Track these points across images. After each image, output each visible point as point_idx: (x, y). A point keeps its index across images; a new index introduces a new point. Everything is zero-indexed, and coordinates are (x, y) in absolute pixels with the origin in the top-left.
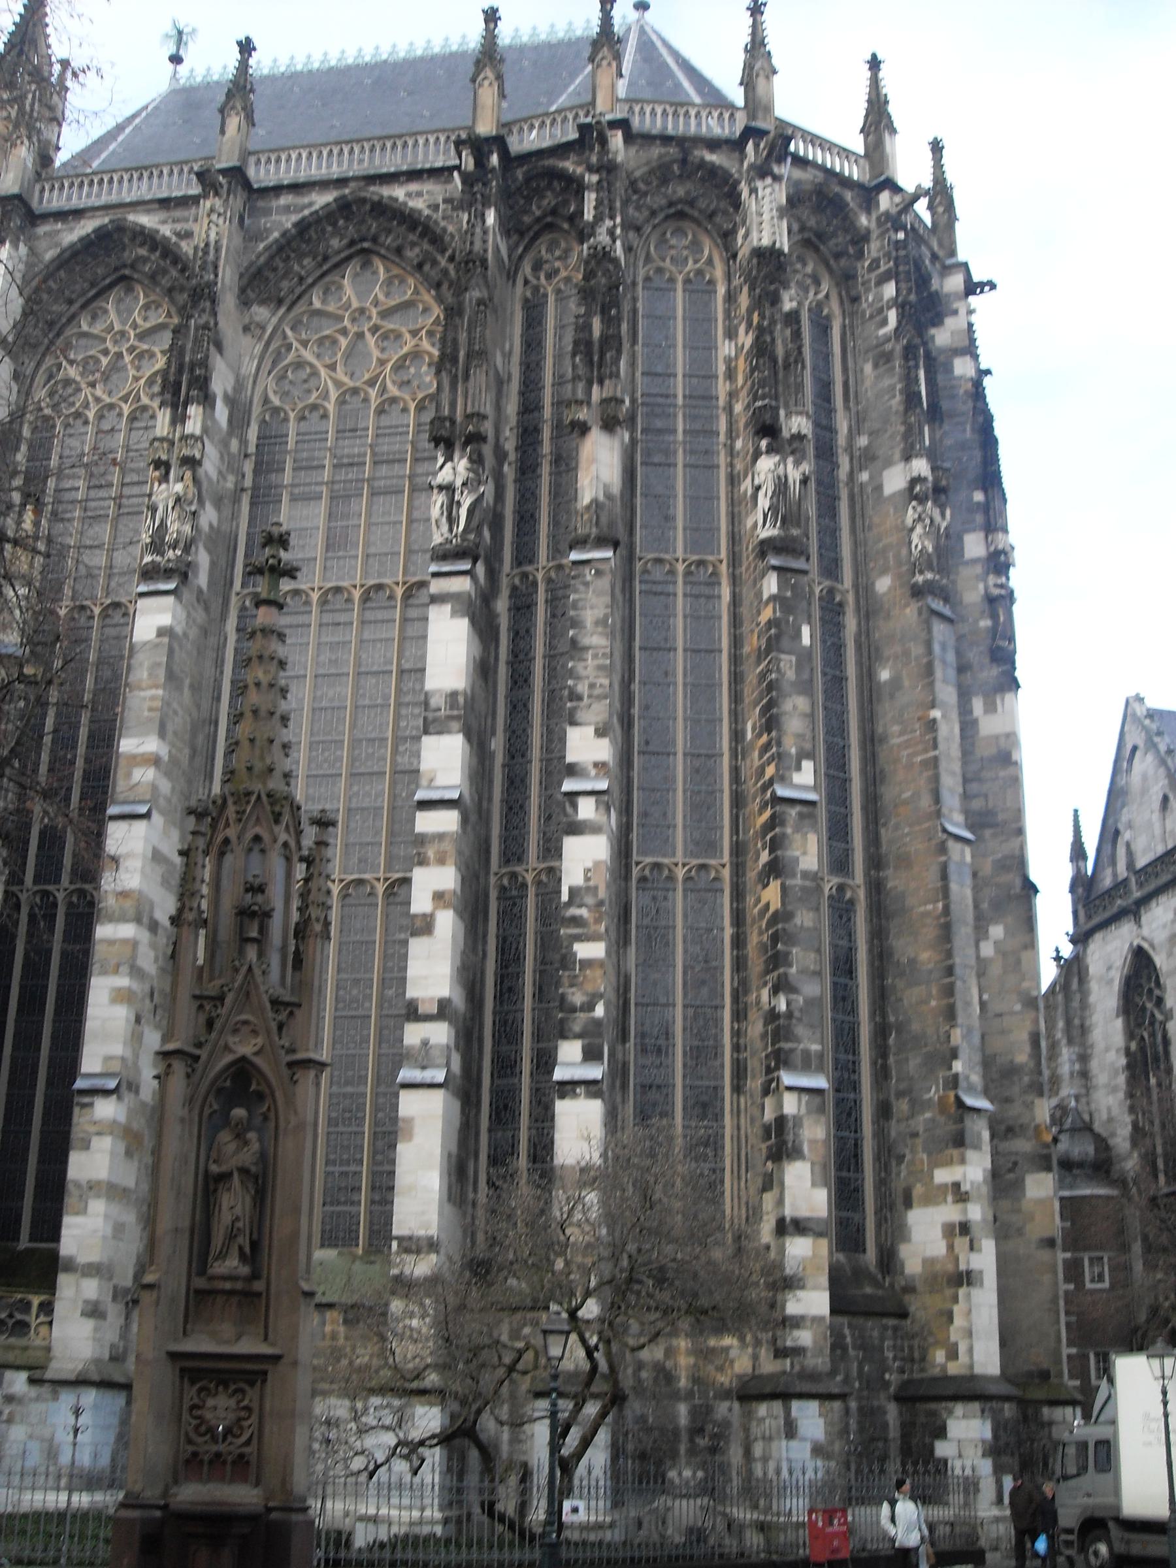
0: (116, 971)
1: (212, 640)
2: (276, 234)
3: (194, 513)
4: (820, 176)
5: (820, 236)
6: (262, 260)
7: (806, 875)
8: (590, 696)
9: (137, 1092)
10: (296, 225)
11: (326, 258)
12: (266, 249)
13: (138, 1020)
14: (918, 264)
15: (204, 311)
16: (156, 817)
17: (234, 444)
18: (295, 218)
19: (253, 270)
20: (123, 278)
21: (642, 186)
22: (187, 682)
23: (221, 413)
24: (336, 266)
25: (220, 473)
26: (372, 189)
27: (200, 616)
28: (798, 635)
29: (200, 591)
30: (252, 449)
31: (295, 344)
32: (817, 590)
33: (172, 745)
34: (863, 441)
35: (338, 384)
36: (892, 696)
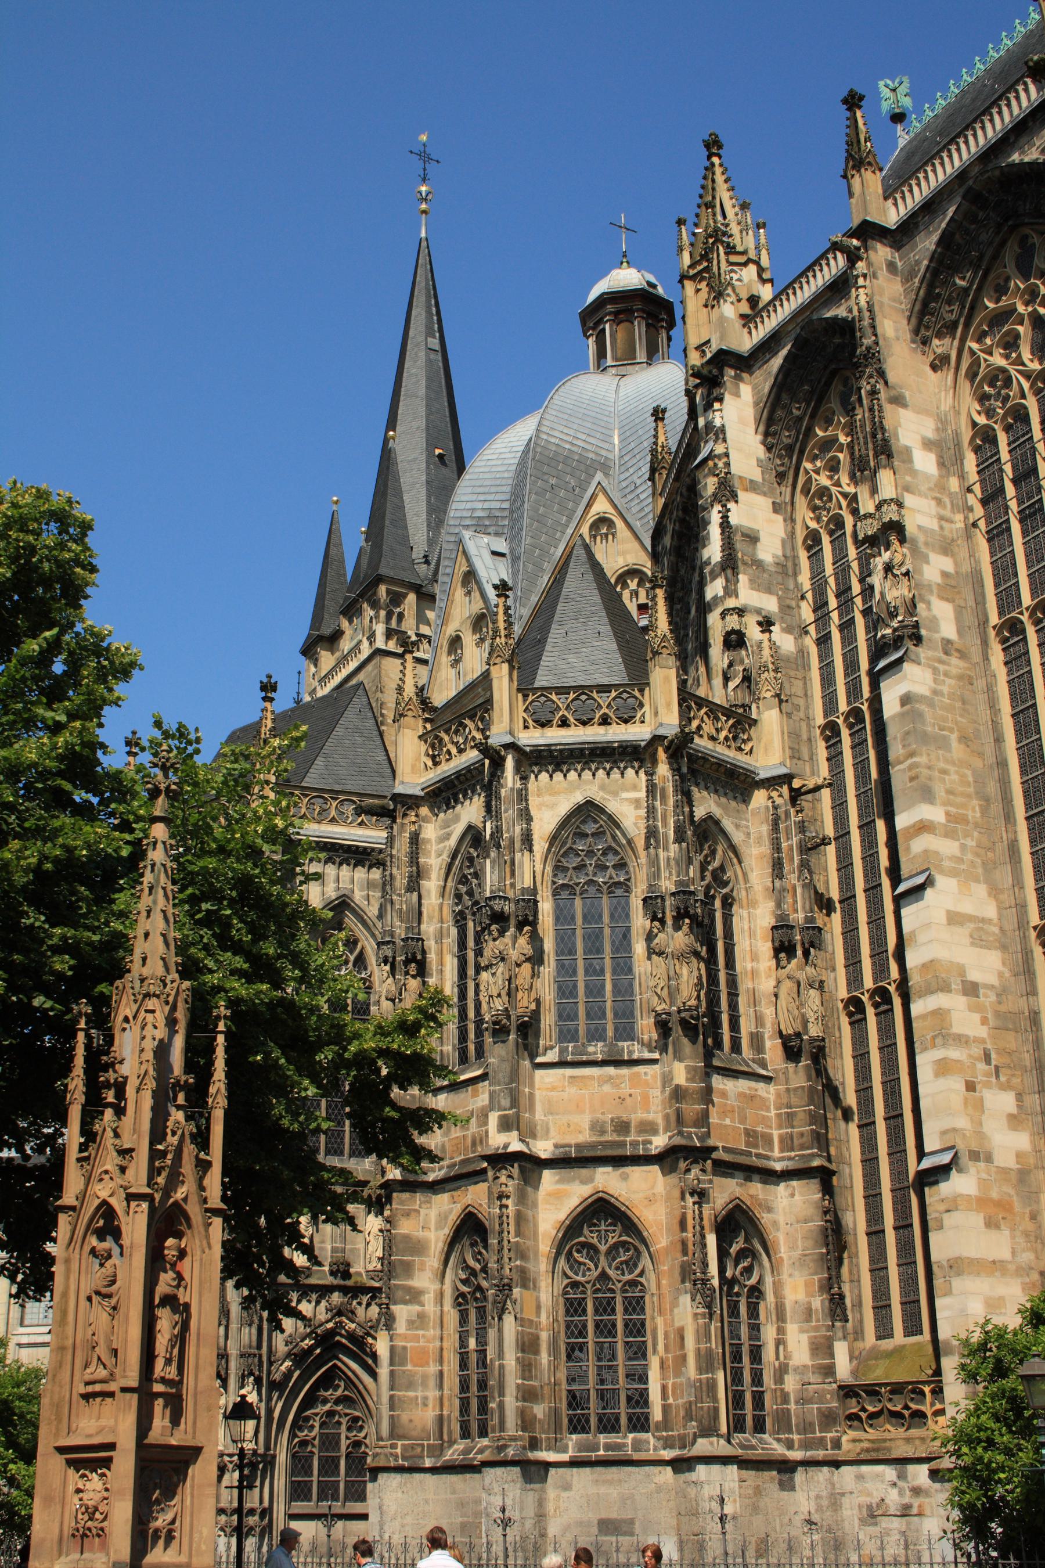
0: (934, 1046)
1: (981, 684)
2: (926, 262)
3: (907, 574)
6: (922, 292)
9: (989, 1159)
10: (939, 243)
11: (981, 258)
12: (921, 282)
13: (970, 1087)
15: (871, 376)
16: (940, 880)
17: (954, 484)
18: (935, 237)
19: (917, 307)
20: (834, 373)
22: (954, 737)
23: (925, 462)
24: (995, 257)
25: (941, 518)
26: (991, 166)
27: (956, 664)
29: (947, 646)
30: (973, 477)
31: (982, 355)
33: (944, 804)
35: (1027, 375)
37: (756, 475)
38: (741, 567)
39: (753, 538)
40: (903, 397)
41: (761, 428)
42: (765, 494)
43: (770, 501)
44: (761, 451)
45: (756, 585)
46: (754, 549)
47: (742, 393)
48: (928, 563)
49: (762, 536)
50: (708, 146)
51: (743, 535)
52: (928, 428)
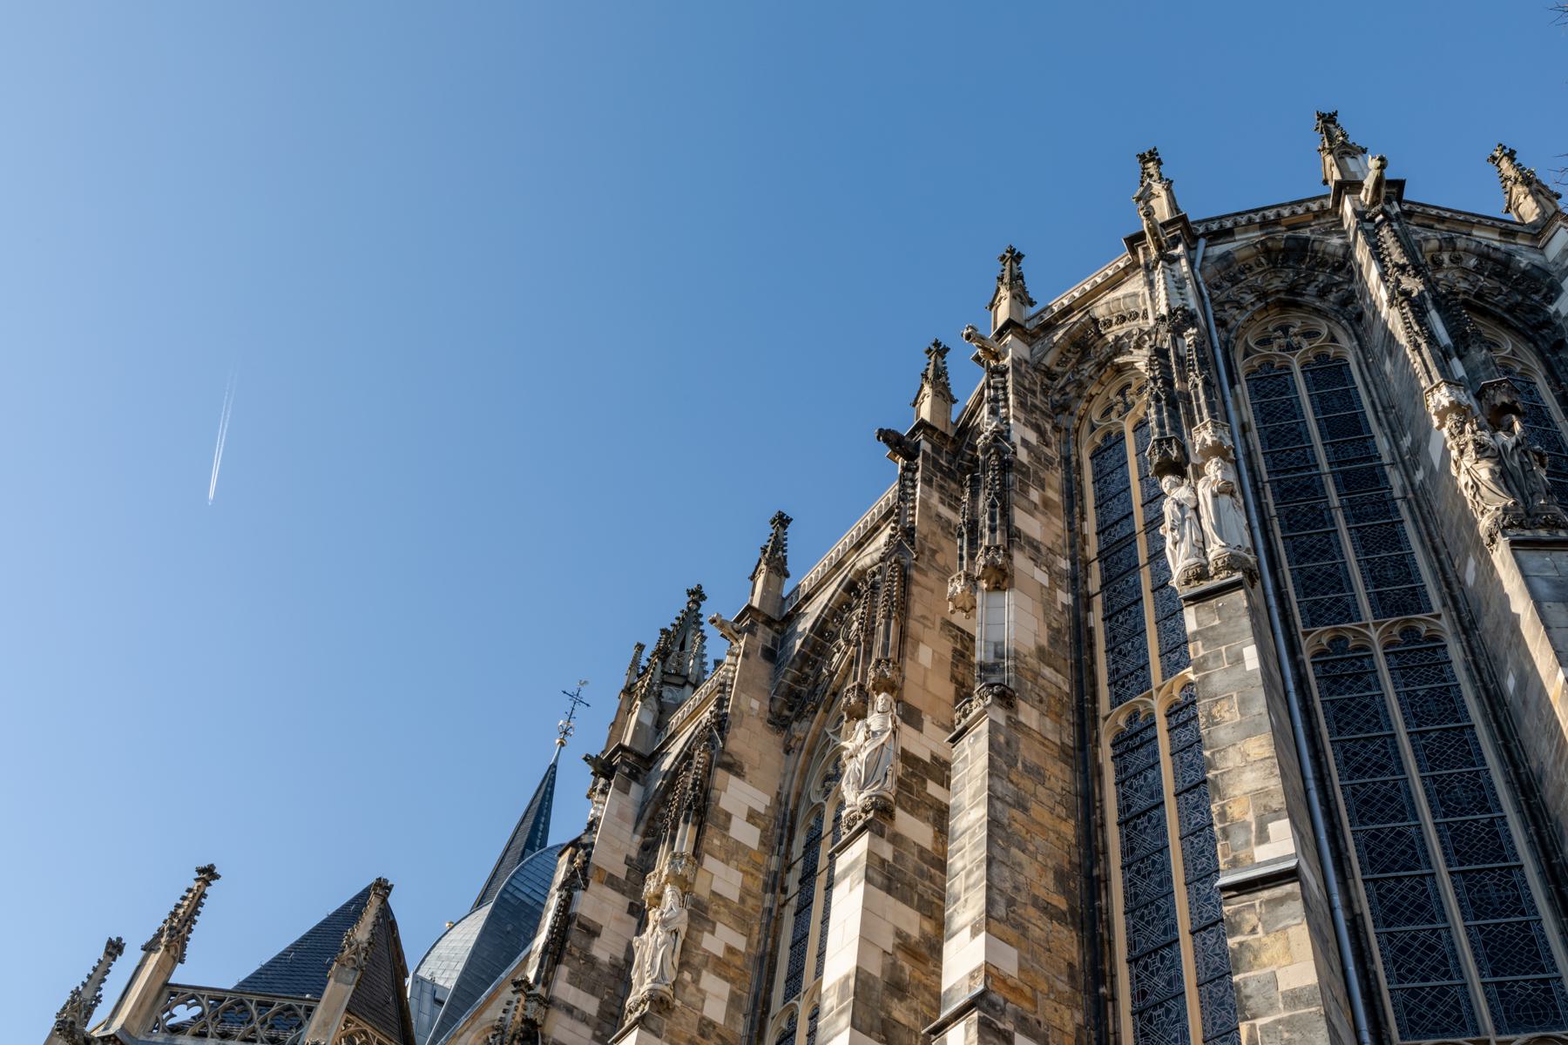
4: (1256, 235)
5: (1292, 289)
7: (1294, 998)
8: (966, 889)
14: (1483, 256)
21: (1059, 369)
23: (746, 834)
28: (1239, 659)
32: (1374, 635)
34: (1406, 442)
36: (1525, 703)
37: (621, 871)
38: (566, 958)
39: (592, 932)
40: (742, 768)
41: (642, 828)
42: (623, 893)
43: (628, 901)
44: (634, 854)
45: (574, 980)
46: (590, 943)
47: (631, 791)
48: (713, 933)
49: (603, 933)
50: (690, 593)
51: (580, 924)
52: (761, 801)
